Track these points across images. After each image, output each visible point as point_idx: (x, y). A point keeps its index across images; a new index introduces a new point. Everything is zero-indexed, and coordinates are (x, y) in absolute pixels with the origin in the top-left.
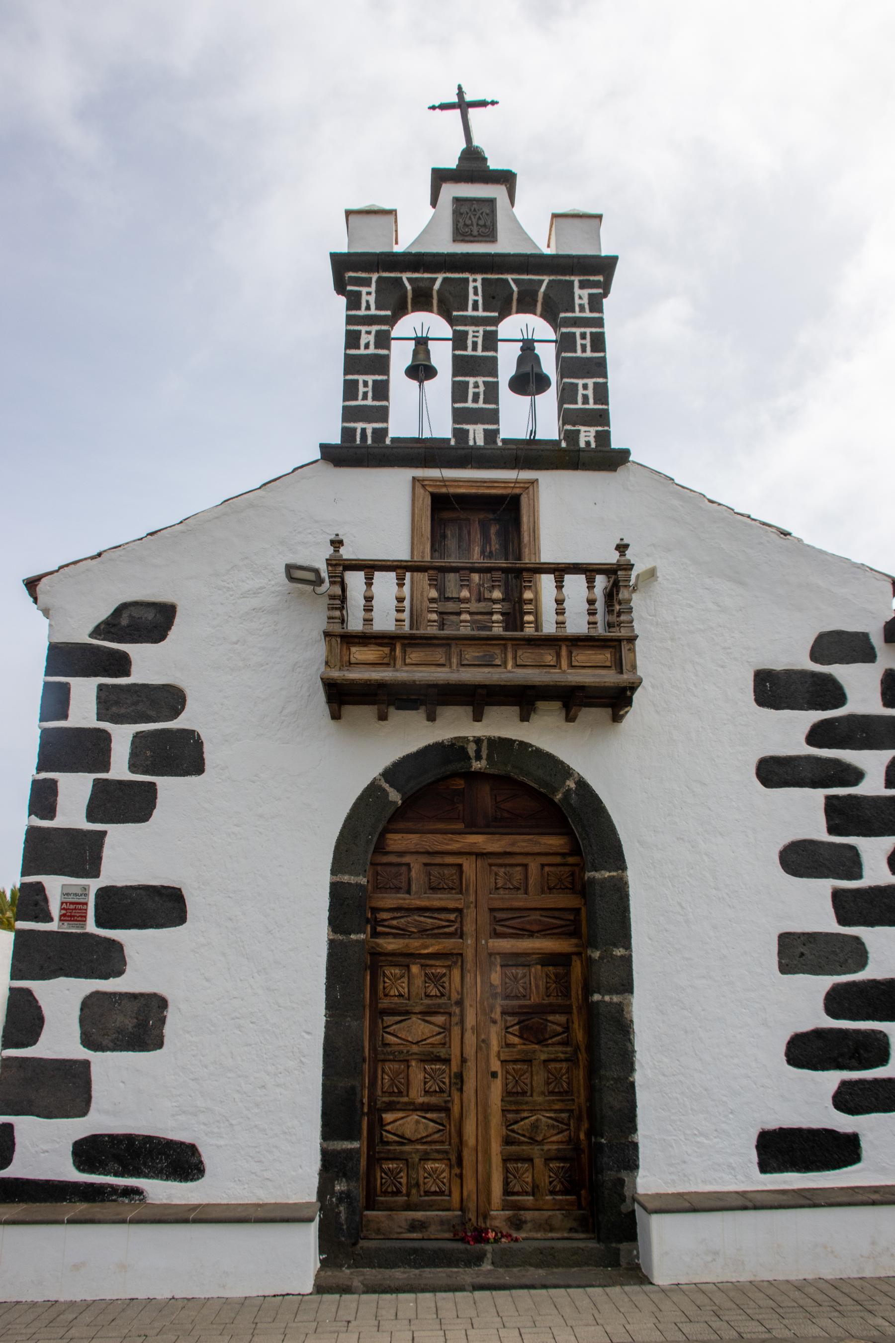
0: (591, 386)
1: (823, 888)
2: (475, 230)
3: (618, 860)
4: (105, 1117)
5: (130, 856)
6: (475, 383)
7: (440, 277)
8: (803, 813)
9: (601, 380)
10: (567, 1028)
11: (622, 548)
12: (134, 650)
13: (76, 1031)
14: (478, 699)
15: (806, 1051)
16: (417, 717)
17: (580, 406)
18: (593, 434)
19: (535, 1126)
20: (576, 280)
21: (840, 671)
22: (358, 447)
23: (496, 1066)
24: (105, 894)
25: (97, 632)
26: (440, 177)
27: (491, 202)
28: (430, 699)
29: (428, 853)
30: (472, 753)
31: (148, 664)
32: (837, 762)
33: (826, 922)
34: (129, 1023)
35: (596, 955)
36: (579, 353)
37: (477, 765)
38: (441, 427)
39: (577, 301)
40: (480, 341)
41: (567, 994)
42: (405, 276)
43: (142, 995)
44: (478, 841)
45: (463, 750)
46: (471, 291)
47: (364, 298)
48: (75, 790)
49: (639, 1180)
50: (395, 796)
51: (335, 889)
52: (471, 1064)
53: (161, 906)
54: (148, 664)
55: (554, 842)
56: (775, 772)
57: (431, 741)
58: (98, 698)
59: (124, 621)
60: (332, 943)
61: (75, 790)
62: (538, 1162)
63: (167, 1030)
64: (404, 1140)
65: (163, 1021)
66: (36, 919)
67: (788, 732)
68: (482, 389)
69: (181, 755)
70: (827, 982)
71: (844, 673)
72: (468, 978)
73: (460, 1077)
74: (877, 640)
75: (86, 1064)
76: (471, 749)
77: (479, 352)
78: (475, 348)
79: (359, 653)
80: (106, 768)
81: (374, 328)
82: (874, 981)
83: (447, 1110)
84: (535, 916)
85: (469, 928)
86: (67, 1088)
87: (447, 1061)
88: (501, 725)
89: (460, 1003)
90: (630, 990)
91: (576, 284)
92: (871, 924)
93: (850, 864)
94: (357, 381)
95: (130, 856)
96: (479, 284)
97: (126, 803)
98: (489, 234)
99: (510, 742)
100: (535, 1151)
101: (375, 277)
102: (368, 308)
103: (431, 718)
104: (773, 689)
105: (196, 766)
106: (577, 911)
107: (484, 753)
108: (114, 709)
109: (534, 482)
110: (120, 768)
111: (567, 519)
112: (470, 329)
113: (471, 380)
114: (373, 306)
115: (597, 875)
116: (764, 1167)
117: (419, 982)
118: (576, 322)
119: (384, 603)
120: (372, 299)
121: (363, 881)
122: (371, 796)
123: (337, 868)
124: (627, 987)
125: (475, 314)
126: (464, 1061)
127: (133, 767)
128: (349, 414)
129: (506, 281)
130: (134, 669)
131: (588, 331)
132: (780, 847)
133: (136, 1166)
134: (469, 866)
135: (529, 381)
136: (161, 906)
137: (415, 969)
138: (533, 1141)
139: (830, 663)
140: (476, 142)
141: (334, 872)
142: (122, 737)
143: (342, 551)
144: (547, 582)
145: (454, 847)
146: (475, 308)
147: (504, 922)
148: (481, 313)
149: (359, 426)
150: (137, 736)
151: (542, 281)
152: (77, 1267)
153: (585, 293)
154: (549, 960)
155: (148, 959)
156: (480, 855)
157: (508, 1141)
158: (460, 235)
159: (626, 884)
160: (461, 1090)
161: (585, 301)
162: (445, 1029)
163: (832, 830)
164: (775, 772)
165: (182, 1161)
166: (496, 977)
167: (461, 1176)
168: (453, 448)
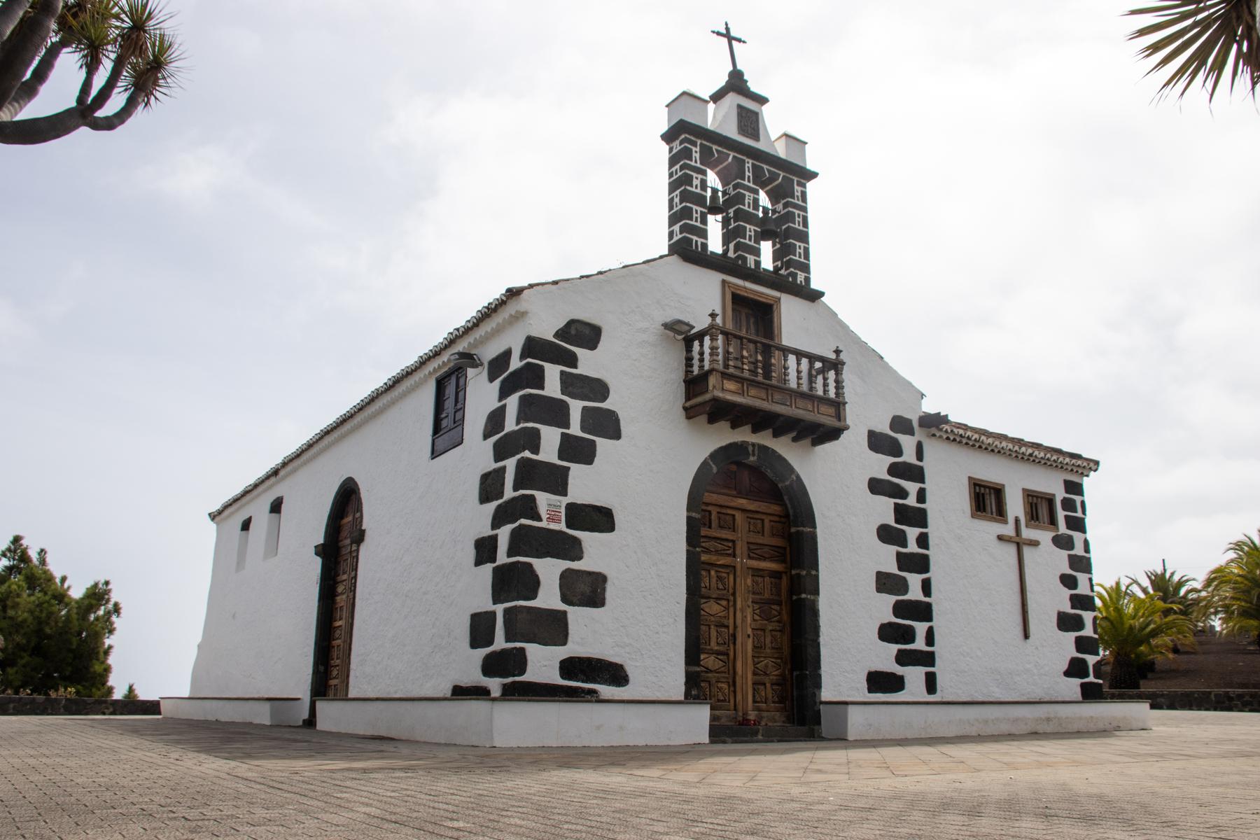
4: (577, 646)
5: (585, 485)
10: (780, 614)
11: (838, 352)
12: (580, 352)
15: (888, 633)
19: (766, 666)
23: (750, 631)
24: (571, 507)
29: (721, 506)
32: (898, 486)
33: (893, 568)
34: (587, 590)
35: (804, 573)
41: (779, 594)
44: (742, 502)
49: (823, 694)
52: (739, 629)
55: (775, 509)
57: (732, 441)
60: (688, 551)
62: (768, 685)
64: (708, 670)
65: (604, 590)
66: (532, 518)
72: (738, 580)
73: (734, 636)
74: (915, 424)
76: (750, 449)
83: (727, 655)
84: (766, 549)
85: (738, 552)
86: (553, 628)
87: (727, 627)
88: (765, 439)
89: (734, 594)
92: (910, 572)
95: (585, 485)
97: (578, 451)
100: (767, 680)
106: (785, 548)
111: (794, 325)
116: (870, 691)
117: (714, 580)
123: (689, 510)
126: (735, 627)
133: (591, 676)
134: (738, 515)
137: (713, 573)
138: (766, 674)
140: (739, 67)
144: (792, 359)
145: (732, 504)
147: (754, 551)
152: (598, 728)
154: (776, 575)
155: (597, 552)
156: (744, 511)
157: (754, 674)
160: (735, 644)
162: (727, 608)
165: (616, 675)
166: (749, 581)
167: (735, 692)
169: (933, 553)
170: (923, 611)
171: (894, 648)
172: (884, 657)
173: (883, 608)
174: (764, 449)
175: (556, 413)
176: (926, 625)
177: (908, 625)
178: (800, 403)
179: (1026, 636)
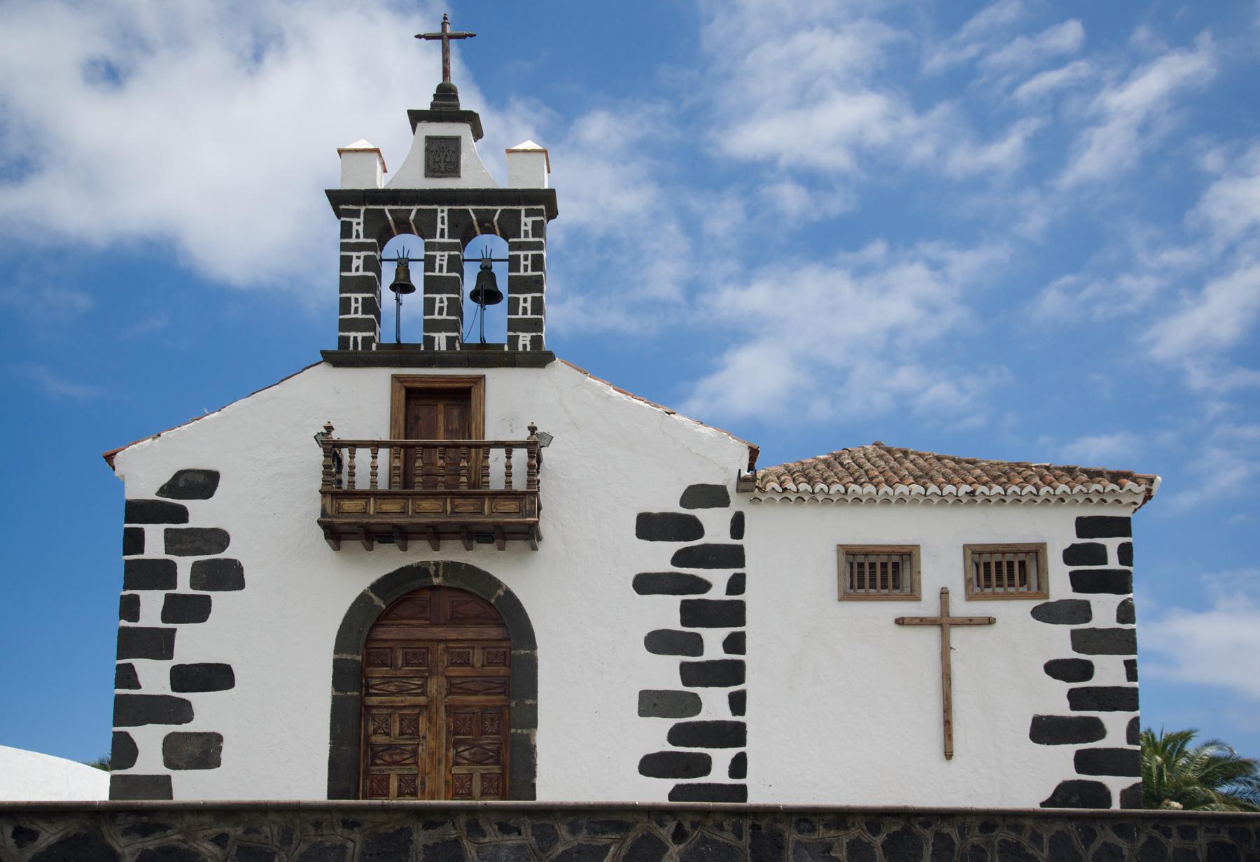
0: (529, 300)
1: (674, 661)
2: (443, 166)
3: (532, 644)
5: (193, 644)
6: (441, 299)
7: (415, 208)
8: (665, 611)
9: (538, 295)
13: (160, 757)
14: (435, 534)
16: (392, 549)
17: (520, 316)
18: (529, 338)
20: (523, 208)
21: (701, 514)
22: (350, 353)
25: (162, 492)
26: (416, 117)
27: (456, 140)
30: (432, 573)
31: (201, 514)
36: (522, 273)
37: (436, 581)
38: (413, 335)
39: (523, 228)
40: (445, 263)
42: (386, 208)
43: (205, 733)
45: (427, 570)
46: (439, 220)
47: (355, 227)
48: (152, 604)
50: (380, 603)
51: (337, 663)
53: (217, 677)
54: (201, 514)
56: (646, 584)
58: (165, 538)
59: (182, 484)
61: (152, 604)
63: (223, 755)
66: (129, 687)
67: (659, 556)
68: (446, 303)
69: (229, 576)
70: (671, 722)
71: (703, 515)
74: (731, 490)
75: (168, 778)
76: (432, 569)
77: (444, 274)
78: (441, 270)
80: (174, 587)
81: (363, 254)
82: (704, 722)
88: (453, 553)
90: (536, 727)
91: (523, 213)
93: (695, 646)
94: (350, 298)
95: (193, 644)
96: (445, 215)
98: (453, 169)
99: (459, 564)
101: (363, 209)
102: (358, 236)
103: (404, 548)
104: (651, 526)
105: (239, 583)
107: (441, 572)
108: (178, 546)
109: (482, 378)
110: (183, 586)
112: (438, 254)
113: (438, 296)
114: (362, 235)
115: (518, 652)
118: (520, 246)
119: (368, 469)
120: (361, 228)
121: (359, 658)
122: (361, 603)
124: (533, 723)
125: (442, 240)
127: (193, 585)
128: (345, 325)
129: (467, 211)
130: (190, 518)
131: (530, 253)
132: (645, 634)
135: (486, 294)
136: (217, 677)
139: (694, 508)
141: (336, 652)
142: (184, 565)
143: (333, 433)
146: (442, 236)
148: (446, 240)
149: (352, 334)
150: (195, 564)
151: (495, 211)
153: (530, 220)
158: (432, 170)
159: (536, 658)
161: (529, 228)
163: (684, 623)
164: (646, 584)
168: (423, 353)
174: (453, 568)
175: (161, 574)
176: (732, 752)
179: (949, 755)
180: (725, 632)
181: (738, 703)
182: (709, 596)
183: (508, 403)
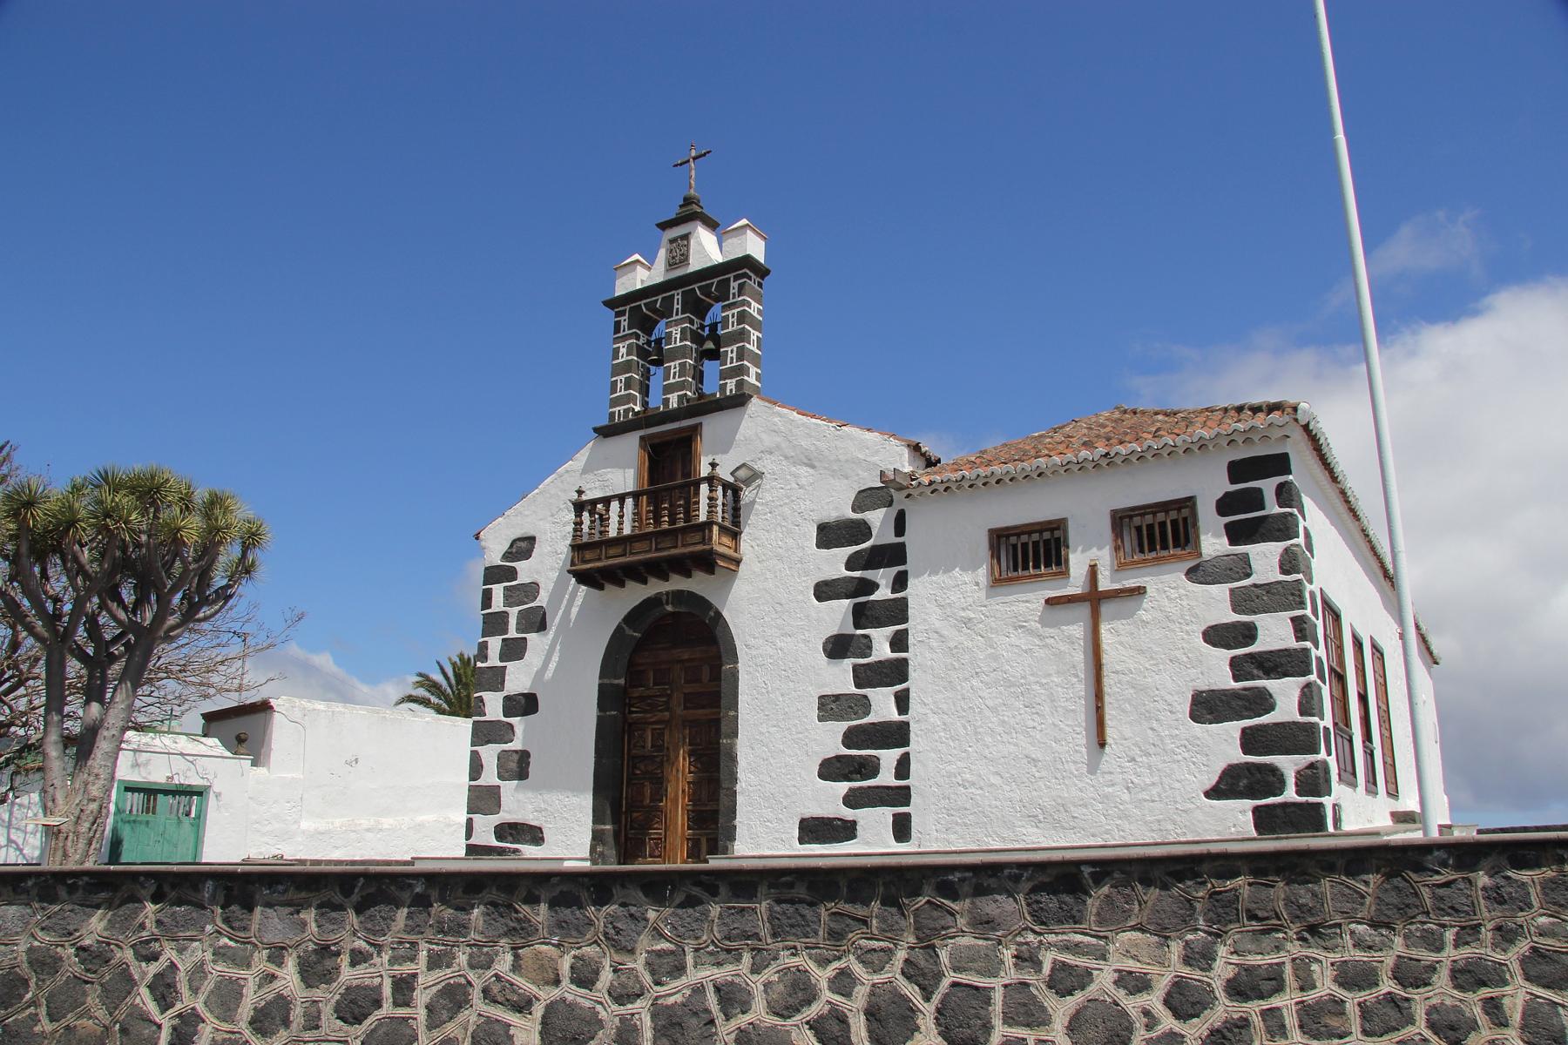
14: (660, 569)
24: (507, 699)
28: (638, 573)
56: (824, 591)
79: (588, 555)
88: (677, 583)
99: (682, 592)
110: (512, 633)
119: (621, 522)
123: (603, 674)
164: (824, 591)
169: (914, 655)
170: (896, 735)
171: (843, 787)
172: (829, 799)
173: (830, 739)
174: (679, 596)
177: (868, 755)
178: (638, 546)
180: (889, 631)
181: (902, 702)
182: (877, 596)
183: (721, 452)
